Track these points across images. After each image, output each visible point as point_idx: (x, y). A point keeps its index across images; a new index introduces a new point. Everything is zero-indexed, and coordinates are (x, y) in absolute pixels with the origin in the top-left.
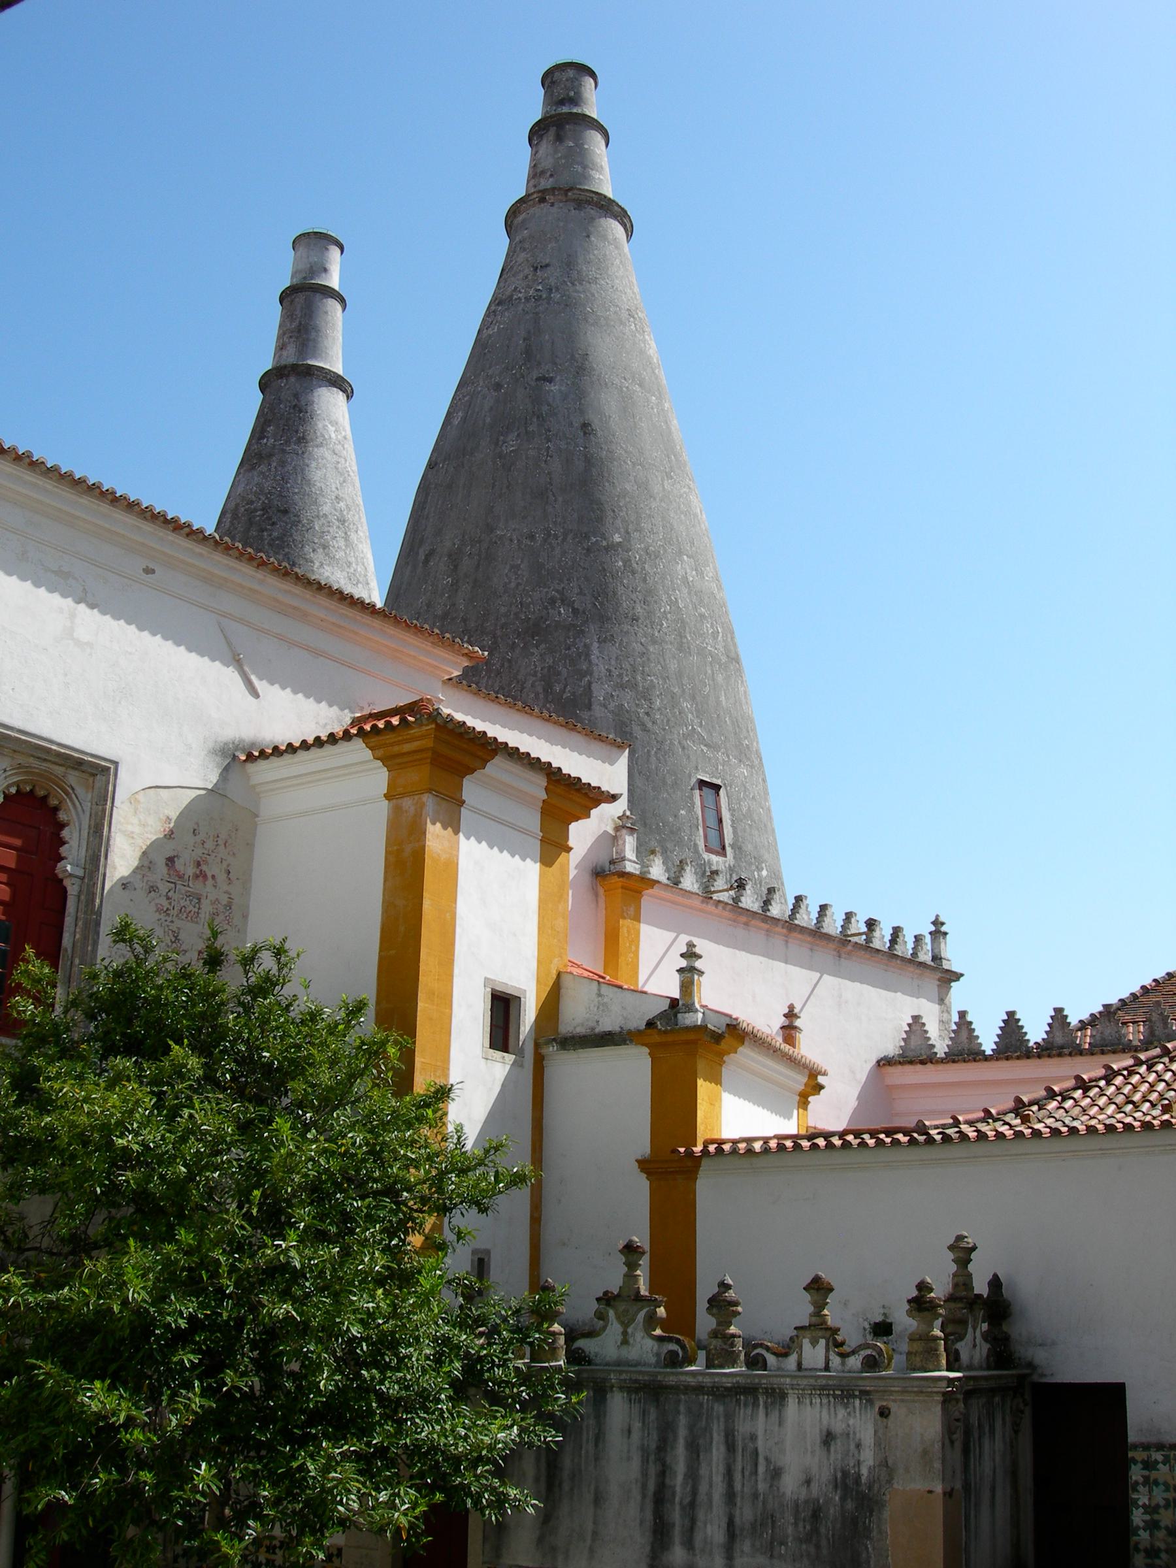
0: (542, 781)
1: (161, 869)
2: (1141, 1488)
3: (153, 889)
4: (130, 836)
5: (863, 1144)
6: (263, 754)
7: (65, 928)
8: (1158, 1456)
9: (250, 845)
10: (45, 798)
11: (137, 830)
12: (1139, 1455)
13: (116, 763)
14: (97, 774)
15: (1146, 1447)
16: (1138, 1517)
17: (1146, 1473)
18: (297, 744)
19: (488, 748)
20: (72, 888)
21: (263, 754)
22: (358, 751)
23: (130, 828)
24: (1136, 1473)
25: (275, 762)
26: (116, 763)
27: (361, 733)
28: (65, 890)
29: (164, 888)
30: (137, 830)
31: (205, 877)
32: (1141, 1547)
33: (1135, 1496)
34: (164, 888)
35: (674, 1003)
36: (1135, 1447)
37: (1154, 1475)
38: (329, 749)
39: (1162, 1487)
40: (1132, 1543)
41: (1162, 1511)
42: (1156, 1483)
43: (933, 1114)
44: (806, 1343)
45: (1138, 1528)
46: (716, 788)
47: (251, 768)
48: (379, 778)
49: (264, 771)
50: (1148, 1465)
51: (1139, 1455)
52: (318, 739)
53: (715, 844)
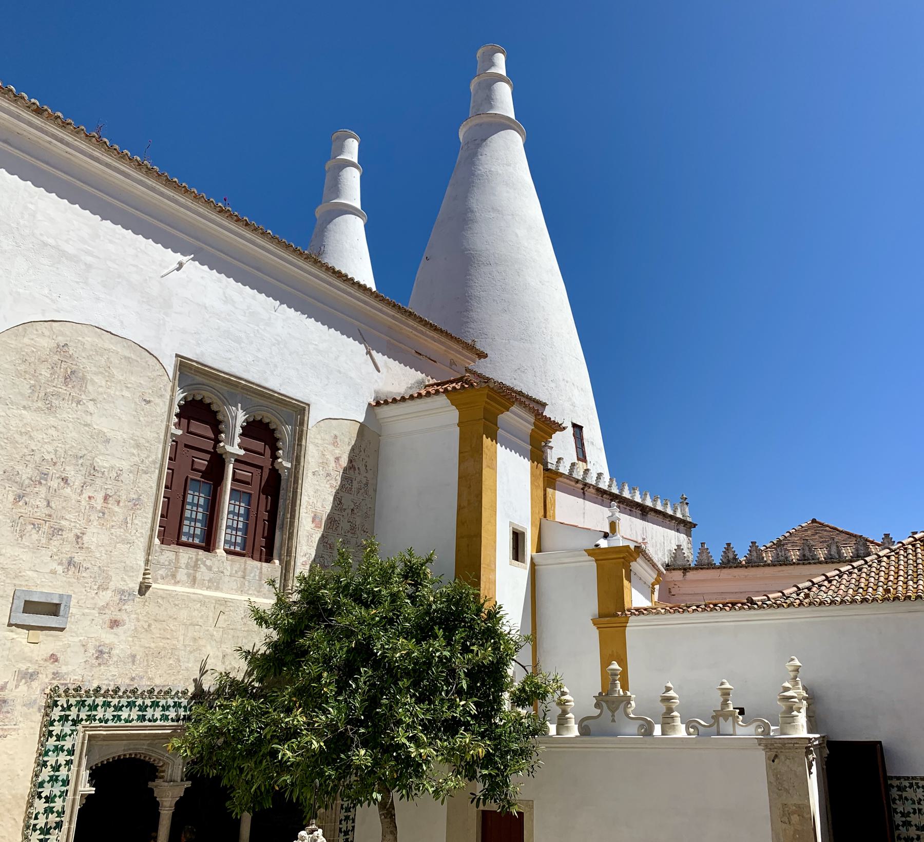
0: (532, 419)
2: (898, 802)
4: (316, 445)
7: (281, 497)
8: (907, 783)
9: (377, 451)
11: (320, 442)
12: (895, 783)
15: (898, 778)
16: (898, 819)
17: (900, 793)
18: (398, 398)
20: (284, 474)
23: (316, 441)
24: (895, 793)
28: (280, 476)
30: (320, 442)
32: (902, 836)
33: (894, 806)
36: (891, 778)
37: (904, 794)
38: (419, 401)
39: (910, 802)
40: (896, 835)
41: (912, 815)
42: (906, 799)
43: (758, 593)
45: (899, 825)
48: (452, 415)
50: (901, 789)
51: (895, 783)
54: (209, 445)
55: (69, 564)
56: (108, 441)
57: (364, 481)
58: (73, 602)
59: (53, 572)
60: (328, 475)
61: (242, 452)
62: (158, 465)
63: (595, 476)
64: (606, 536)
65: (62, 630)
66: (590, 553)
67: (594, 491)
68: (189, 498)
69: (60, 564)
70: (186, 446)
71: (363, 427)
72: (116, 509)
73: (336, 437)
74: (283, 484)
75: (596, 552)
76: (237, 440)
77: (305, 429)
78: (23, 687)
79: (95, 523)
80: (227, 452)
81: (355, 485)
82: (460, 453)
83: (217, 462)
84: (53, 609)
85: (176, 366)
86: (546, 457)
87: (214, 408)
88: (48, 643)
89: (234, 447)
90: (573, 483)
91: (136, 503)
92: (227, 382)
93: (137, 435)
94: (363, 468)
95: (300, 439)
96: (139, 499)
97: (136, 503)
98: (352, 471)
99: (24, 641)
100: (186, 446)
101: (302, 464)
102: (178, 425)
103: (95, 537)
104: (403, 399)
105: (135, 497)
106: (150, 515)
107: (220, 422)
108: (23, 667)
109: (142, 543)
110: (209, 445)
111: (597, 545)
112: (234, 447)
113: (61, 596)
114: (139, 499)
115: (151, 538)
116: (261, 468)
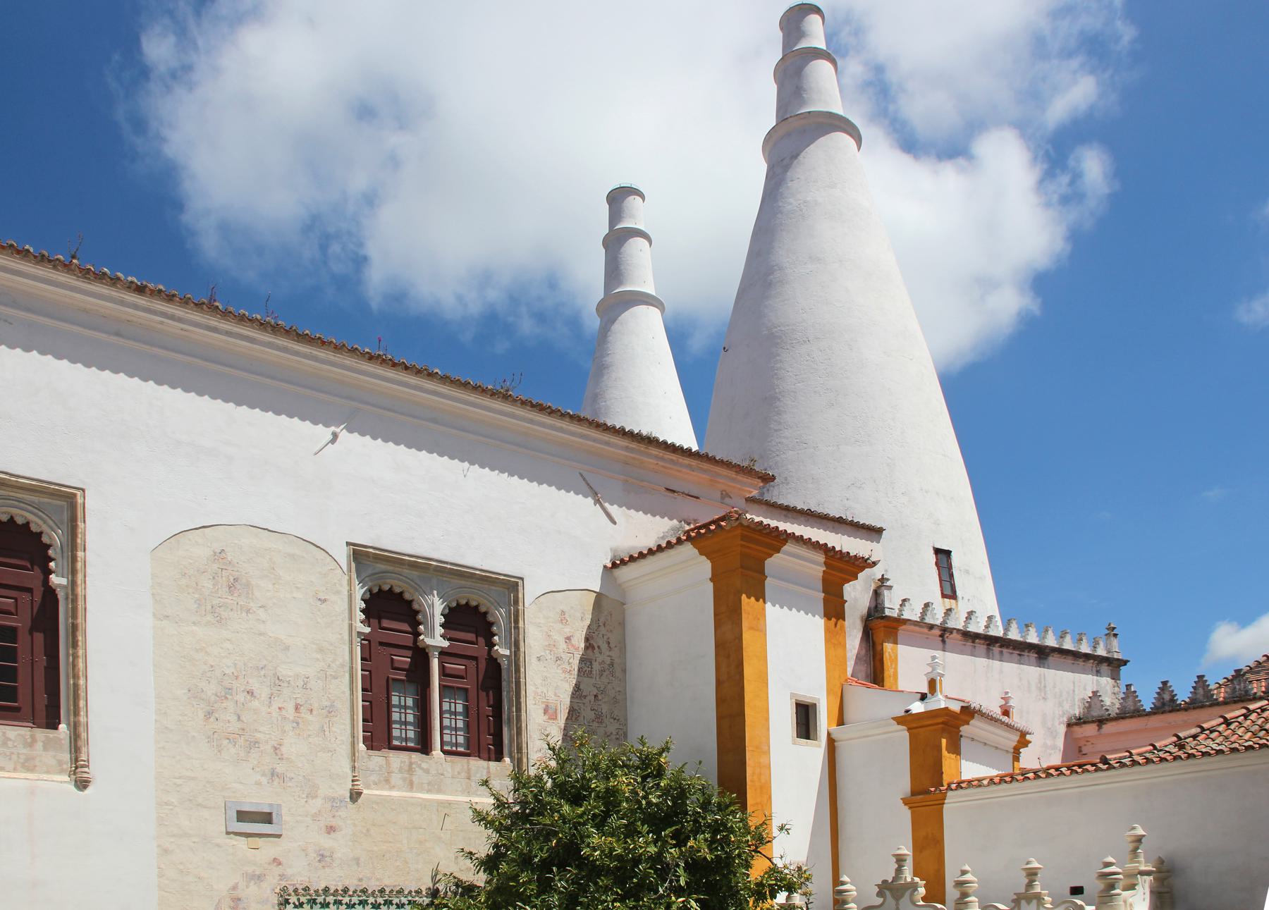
1: (563, 646)
3: (558, 659)
5: (1062, 773)
6: (623, 562)
9: (622, 624)
10: (477, 607)
13: (522, 579)
14: (510, 587)
19: (779, 539)
20: (504, 663)
21: (623, 562)
22: (688, 550)
25: (633, 566)
26: (522, 579)
27: (689, 539)
28: (499, 666)
29: (565, 657)
31: (593, 648)
34: (565, 657)
35: (923, 697)
44: (1023, 903)
46: (948, 553)
47: (617, 572)
49: (624, 573)
52: (659, 547)
53: (948, 592)
54: (408, 639)
55: (273, 775)
56: (287, 648)
57: (608, 661)
58: (284, 810)
59: (258, 783)
60: (558, 659)
61: (446, 644)
62: (347, 669)
63: (963, 616)
64: (923, 697)
65: (279, 836)
66: (899, 720)
67: (959, 637)
68: (395, 700)
69: (264, 775)
70: (381, 644)
71: (599, 597)
72: (310, 717)
73: (563, 612)
74: (504, 675)
75: (907, 720)
76: (439, 630)
77: (521, 607)
78: (253, 888)
79: (291, 734)
80: (428, 646)
81: (596, 666)
82: (715, 615)
83: (421, 656)
84: (267, 818)
85: (349, 556)
86: (883, 601)
87: (407, 596)
88: (268, 849)
89: (435, 638)
90: (926, 630)
91: (331, 711)
92: (414, 566)
93: (324, 637)
94: (604, 646)
95: (517, 621)
96: (332, 706)
97: (331, 711)
98: (590, 651)
99: (245, 847)
100: (381, 644)
101: (522, 649)
102: (367, 622)
103: (293, 746)
104: (651, 552)
105: (328, 703)
106: (348, 721)
107: (417, 612)
108: (250, 869)
109: (345, 749)
110: (408, 639)
111: (907, 711)
112: (435, 638)
113: (271, 805)
114: (332, 706)
115: (353, 745)
116: (475, 658)
